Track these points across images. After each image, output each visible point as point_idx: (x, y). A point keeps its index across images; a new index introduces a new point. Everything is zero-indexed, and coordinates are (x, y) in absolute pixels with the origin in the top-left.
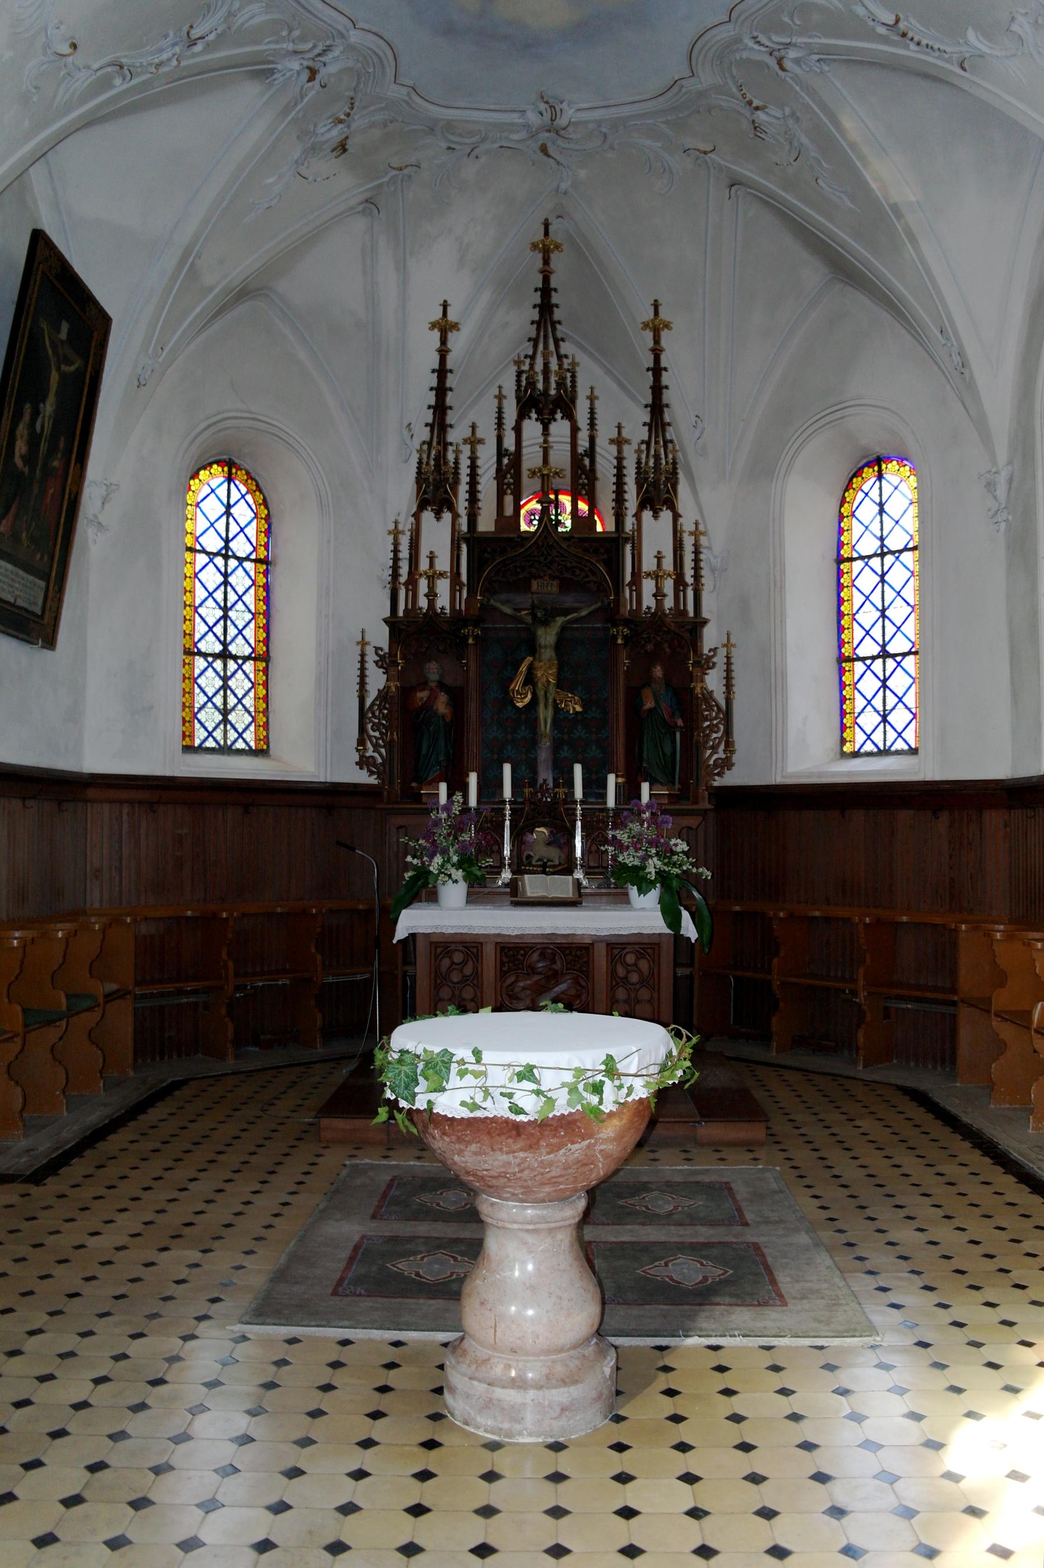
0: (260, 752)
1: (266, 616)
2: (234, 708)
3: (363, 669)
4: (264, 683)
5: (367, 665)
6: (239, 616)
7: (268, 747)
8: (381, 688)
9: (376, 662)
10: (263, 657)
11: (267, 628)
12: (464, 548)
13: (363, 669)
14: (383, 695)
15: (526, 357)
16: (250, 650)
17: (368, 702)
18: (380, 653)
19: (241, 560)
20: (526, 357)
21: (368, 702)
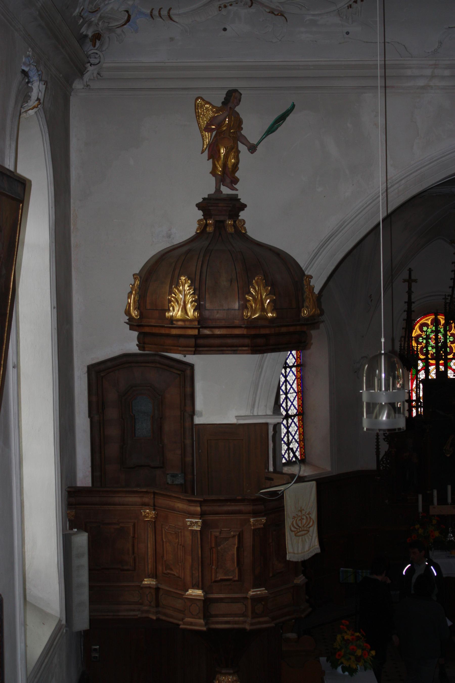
0: (303, 461)
1: (302, 393)
2: (291, 442)
3: (378, 442)
4: (302, 427)
5: (380, 440)
6: (292, 396)
7: (305, 457)
8: (387, 450)
9: (384, 439)
10: (301, 414)
11: (302, 401)
12: (421, 385)
13: (378, 442)
14: (386, 454)
15: (448, 296)
16: (296, 411)
17: (381, 456)
18: (386, 435)
19: (291, 367)
20: (448, 296)
21: (381, 456)
